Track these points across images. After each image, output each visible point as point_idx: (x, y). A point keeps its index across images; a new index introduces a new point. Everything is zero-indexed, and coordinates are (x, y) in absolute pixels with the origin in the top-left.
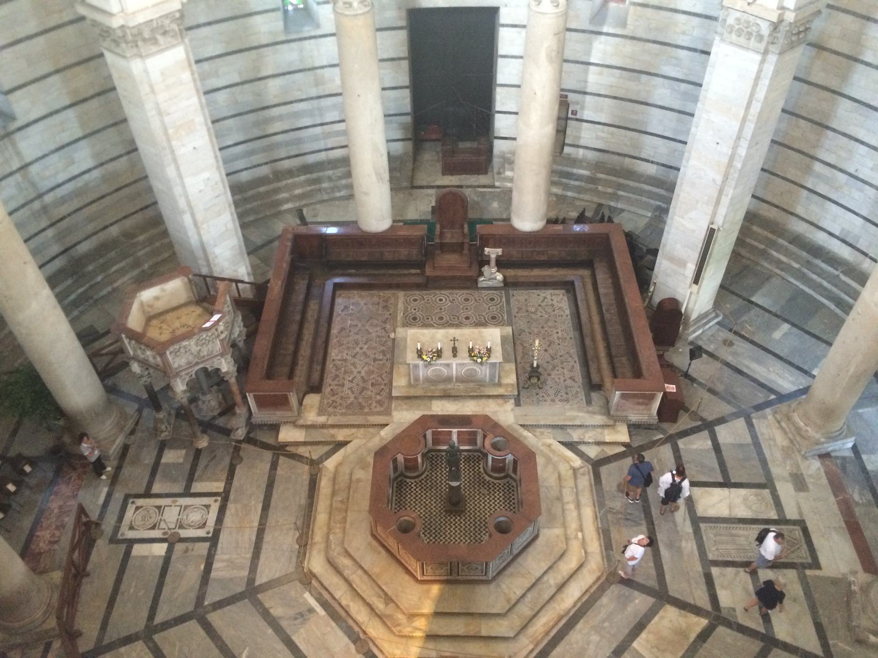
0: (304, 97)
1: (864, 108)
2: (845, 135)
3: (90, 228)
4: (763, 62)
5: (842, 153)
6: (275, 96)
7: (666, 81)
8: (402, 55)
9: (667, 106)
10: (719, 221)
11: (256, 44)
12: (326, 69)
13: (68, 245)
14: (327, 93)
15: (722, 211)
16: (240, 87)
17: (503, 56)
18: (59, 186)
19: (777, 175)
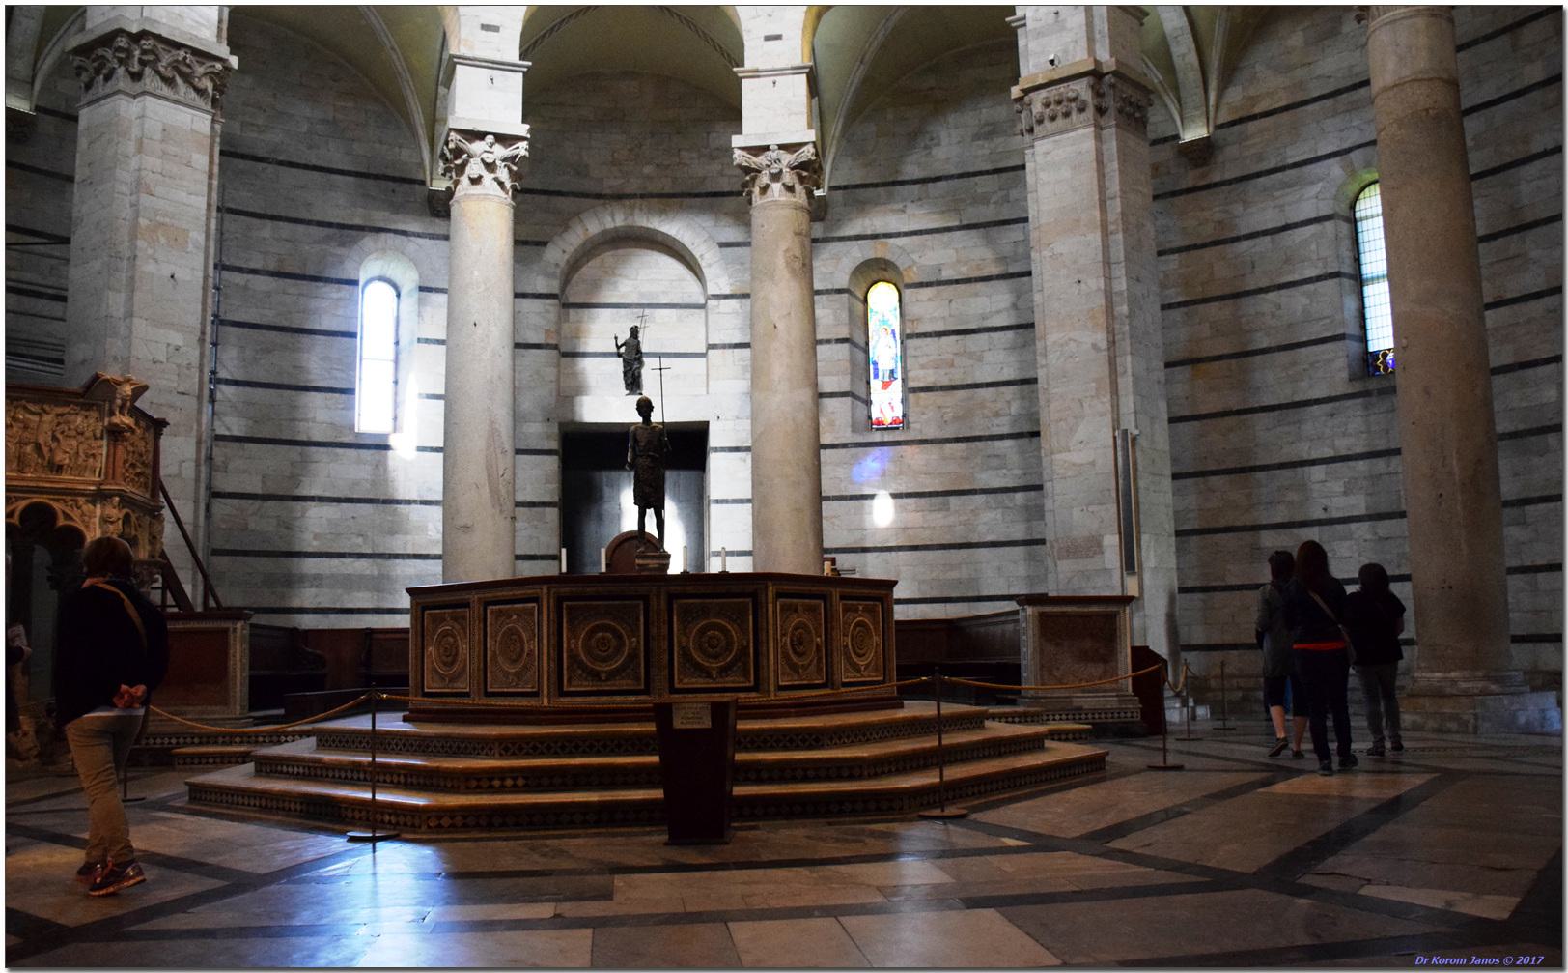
1: (1291, 411)
2: (1282, 466)
4: (1098, 138)
5: (1292, 496)
6: (316, 537)
7: (990, 497)
8: (547, 499)
9: (1003, 539)
10: (1129, 423)
11: (303, 437)
12: (414, 506)
14: (410, 551)
15: (1128, 403)
16: (258, 503)
17: (717, 501)
19: (1214, 589)
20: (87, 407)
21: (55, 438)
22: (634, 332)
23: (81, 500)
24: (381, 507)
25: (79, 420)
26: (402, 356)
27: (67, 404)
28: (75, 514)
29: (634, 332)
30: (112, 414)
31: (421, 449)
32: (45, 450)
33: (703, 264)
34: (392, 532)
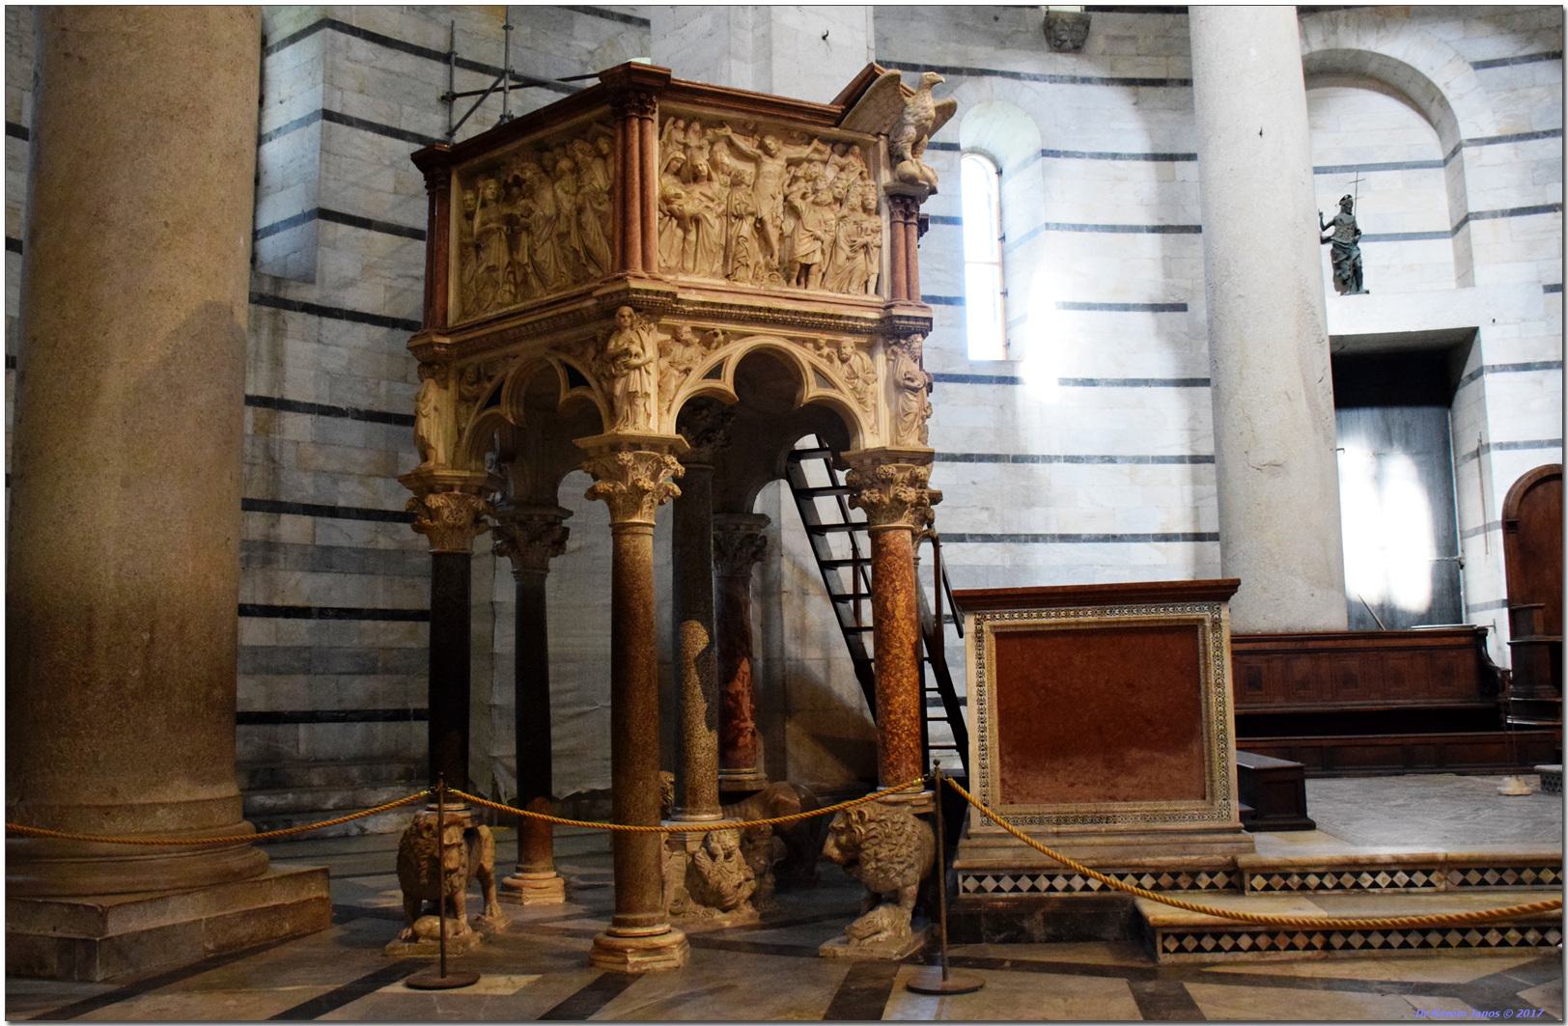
0: (998, 531)
3: (357, 691)
12: (1055, 464)
13: (285, 705)
17: (1501, 446)
18: (333, 512)
20: (845, 147)
21: (792, 210)
22: (1347, 204)
23: (848, 342)
24: (1010, 466)
25: (830, 173)
26: (1009, 257)
27: (809, 138)
28: (837, 372)
29: (1347, 204)
30: (895, 157)
31: (1064, 382)
32: (774, 235)
33: (1450, 96)
34: (1029, 504)
